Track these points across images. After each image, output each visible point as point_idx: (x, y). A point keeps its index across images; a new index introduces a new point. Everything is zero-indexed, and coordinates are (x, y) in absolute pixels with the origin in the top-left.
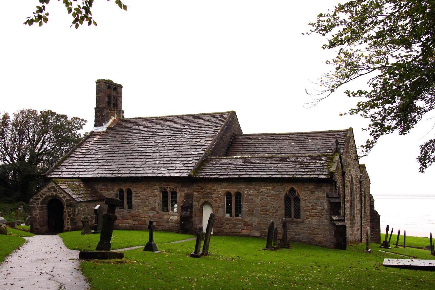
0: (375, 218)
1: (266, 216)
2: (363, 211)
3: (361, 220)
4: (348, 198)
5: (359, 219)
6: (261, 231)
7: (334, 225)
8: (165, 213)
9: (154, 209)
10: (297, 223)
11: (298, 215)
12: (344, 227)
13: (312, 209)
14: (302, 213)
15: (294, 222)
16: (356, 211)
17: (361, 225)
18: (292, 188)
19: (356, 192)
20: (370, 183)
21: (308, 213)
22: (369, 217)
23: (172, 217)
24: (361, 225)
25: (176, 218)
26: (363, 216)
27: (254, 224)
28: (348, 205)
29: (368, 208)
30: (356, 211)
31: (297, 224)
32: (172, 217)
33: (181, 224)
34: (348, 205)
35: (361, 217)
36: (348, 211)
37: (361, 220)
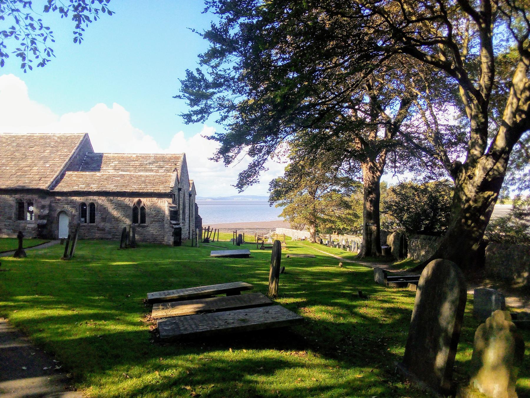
0: (198, 221)
1: (117, 222)
2: (191, 216)
3: (190, 223)
4: (181, 207)
5: (188, 222)
6: (113, 235)
7: (173, 227)
8: (21, 221)
9: (10, 218)
10: (143, 227)
11: (143, 221)
12: (180, 229)
13: (156, 216)
14: (147, 219)
15: (141, 226)
16: (187, 216)
17: (189, 226)
18: (140, 200)
19: (187, 201)
20: (196, 194)
21: (152, 219)
22: (194, 221)
23: (28, 225)
24: (189, 226)
25: (33, 226)
26: (191, 220)
27: (107, 229)
28: (181, 212)
29: (194, 213)
30: (187, 216)
31: (143, 228)
32: (28, 225)
33: (38, 231)
34: (181, 212)
35: (189, 221)
36: (181, 217)
37: (190, 223)
